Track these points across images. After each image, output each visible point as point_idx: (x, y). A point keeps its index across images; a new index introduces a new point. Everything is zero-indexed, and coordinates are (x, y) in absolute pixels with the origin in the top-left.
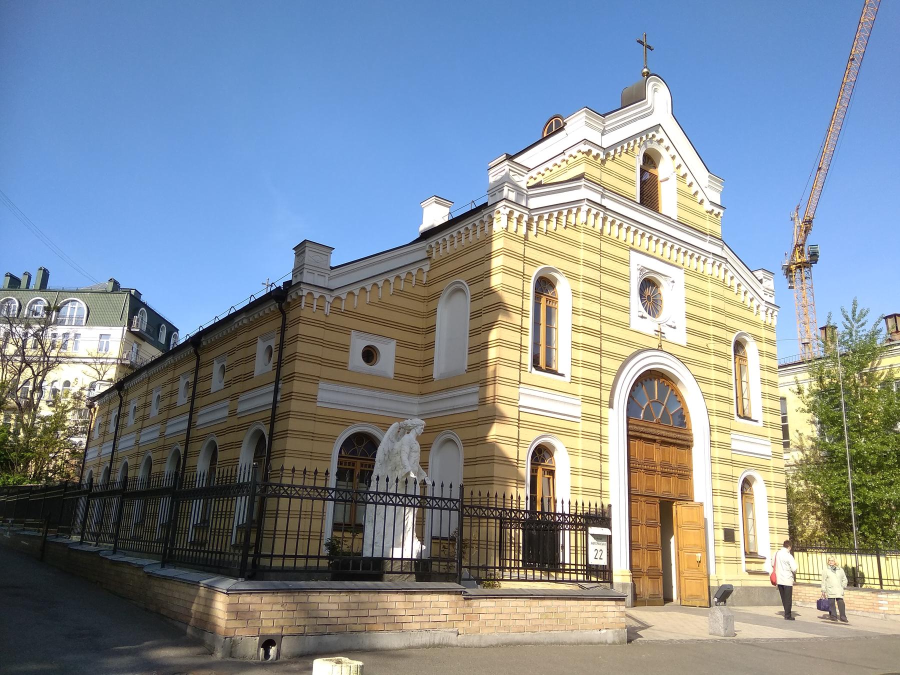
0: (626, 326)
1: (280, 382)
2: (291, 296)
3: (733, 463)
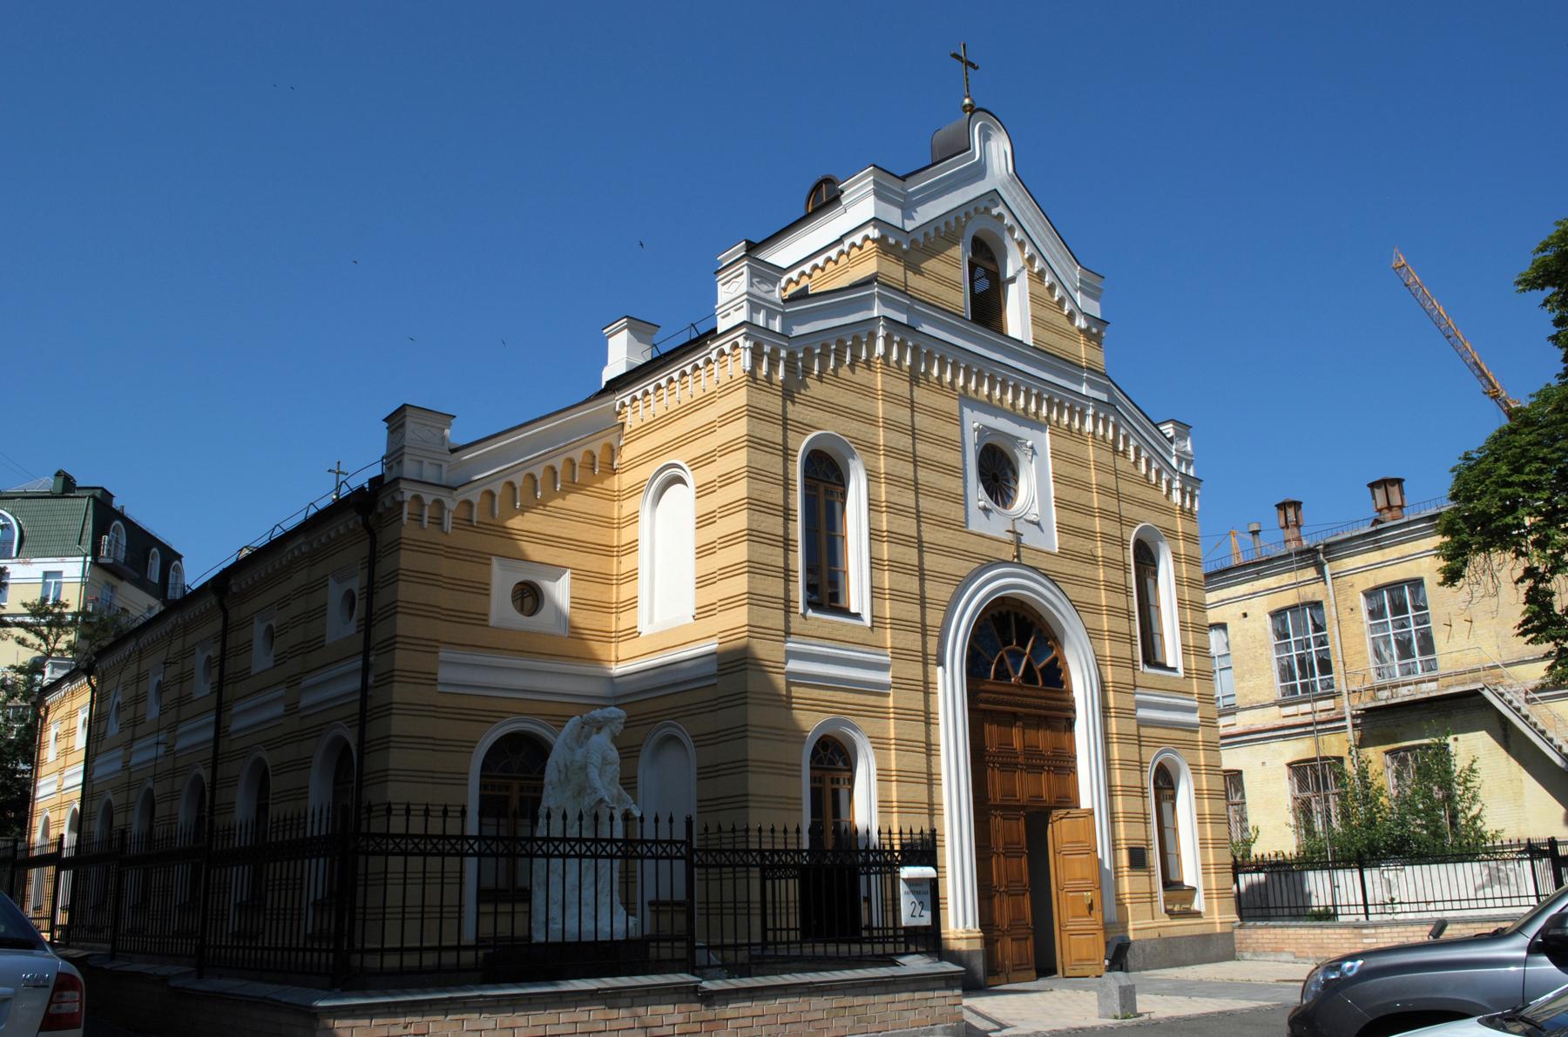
1: (372, 652)
2: (383, 503)
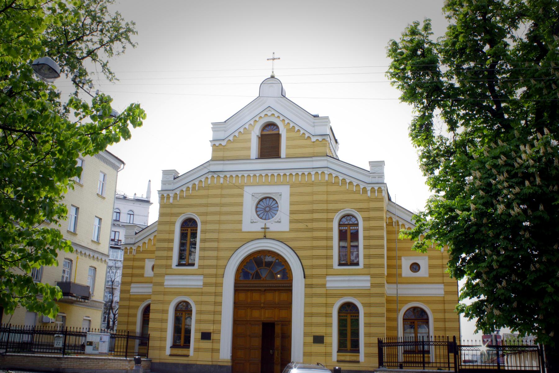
0: (240, 231)
3: (327, 295)
